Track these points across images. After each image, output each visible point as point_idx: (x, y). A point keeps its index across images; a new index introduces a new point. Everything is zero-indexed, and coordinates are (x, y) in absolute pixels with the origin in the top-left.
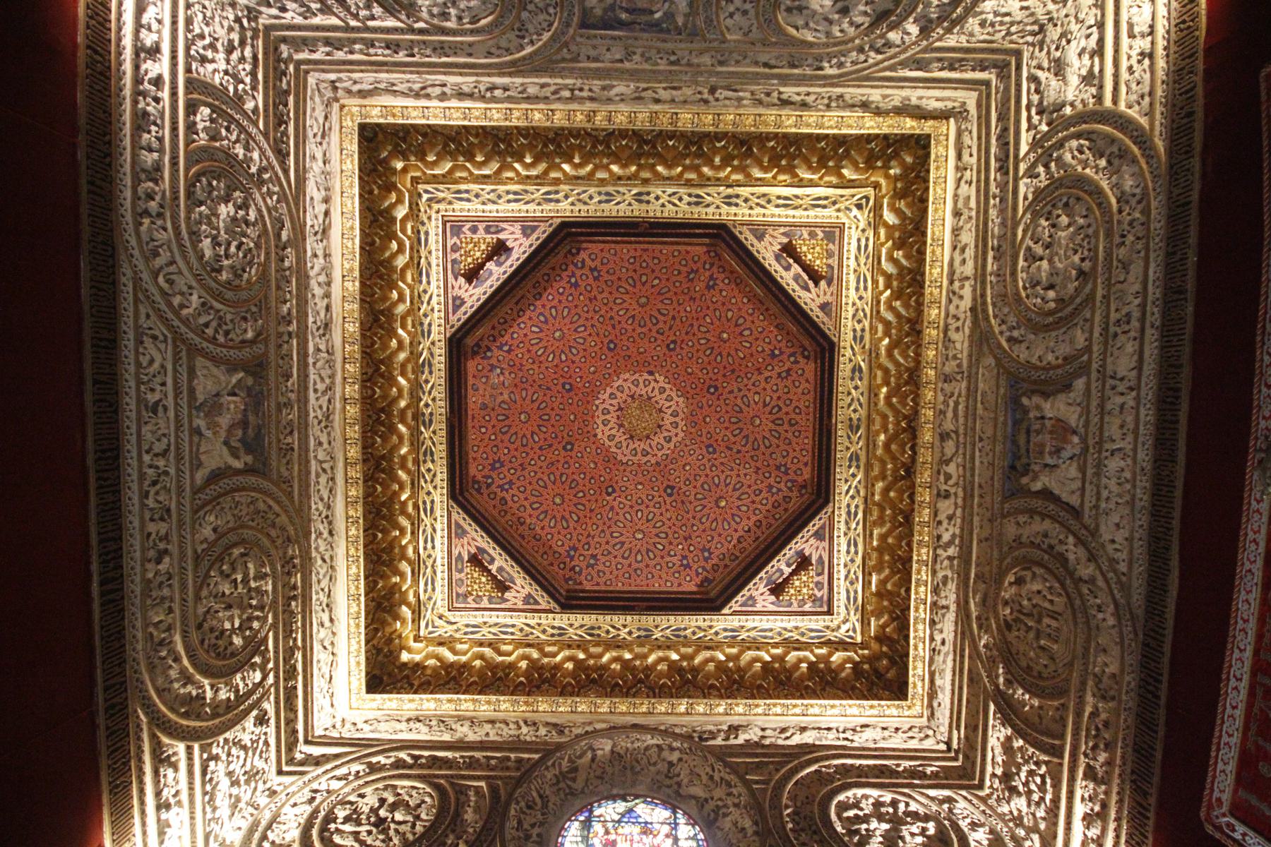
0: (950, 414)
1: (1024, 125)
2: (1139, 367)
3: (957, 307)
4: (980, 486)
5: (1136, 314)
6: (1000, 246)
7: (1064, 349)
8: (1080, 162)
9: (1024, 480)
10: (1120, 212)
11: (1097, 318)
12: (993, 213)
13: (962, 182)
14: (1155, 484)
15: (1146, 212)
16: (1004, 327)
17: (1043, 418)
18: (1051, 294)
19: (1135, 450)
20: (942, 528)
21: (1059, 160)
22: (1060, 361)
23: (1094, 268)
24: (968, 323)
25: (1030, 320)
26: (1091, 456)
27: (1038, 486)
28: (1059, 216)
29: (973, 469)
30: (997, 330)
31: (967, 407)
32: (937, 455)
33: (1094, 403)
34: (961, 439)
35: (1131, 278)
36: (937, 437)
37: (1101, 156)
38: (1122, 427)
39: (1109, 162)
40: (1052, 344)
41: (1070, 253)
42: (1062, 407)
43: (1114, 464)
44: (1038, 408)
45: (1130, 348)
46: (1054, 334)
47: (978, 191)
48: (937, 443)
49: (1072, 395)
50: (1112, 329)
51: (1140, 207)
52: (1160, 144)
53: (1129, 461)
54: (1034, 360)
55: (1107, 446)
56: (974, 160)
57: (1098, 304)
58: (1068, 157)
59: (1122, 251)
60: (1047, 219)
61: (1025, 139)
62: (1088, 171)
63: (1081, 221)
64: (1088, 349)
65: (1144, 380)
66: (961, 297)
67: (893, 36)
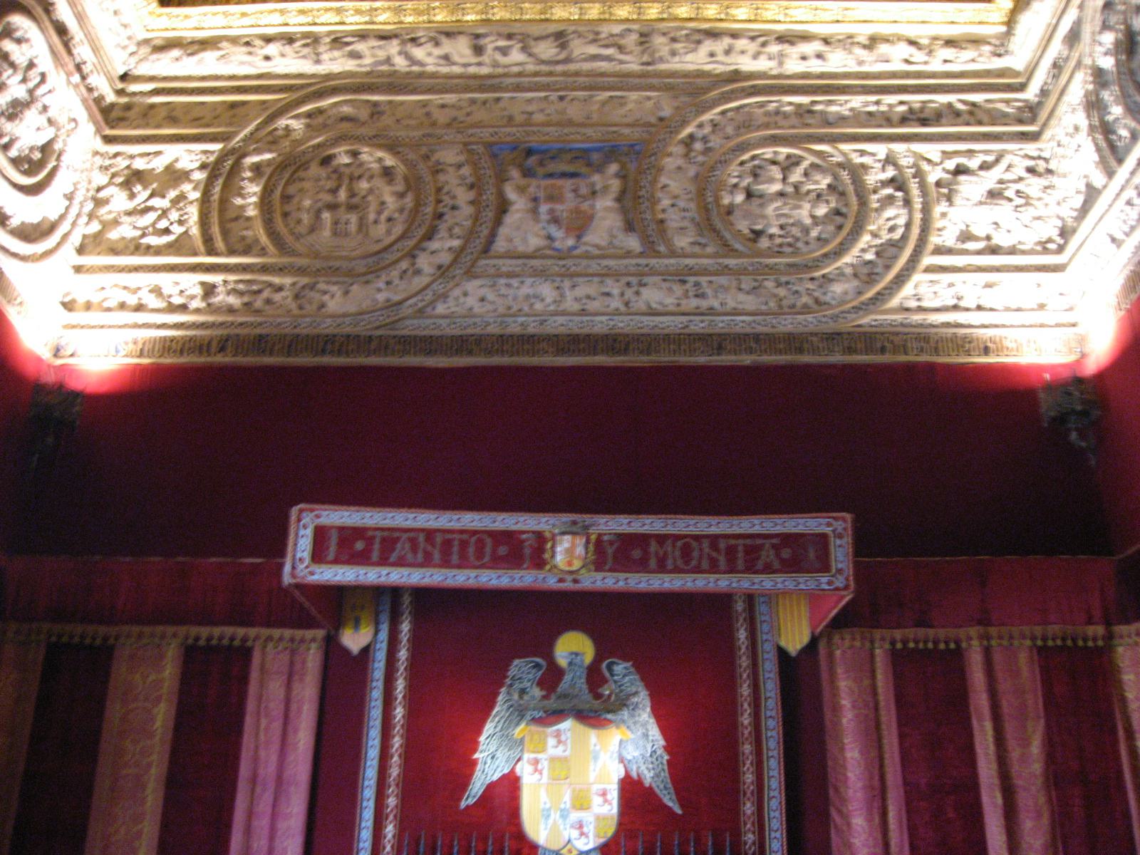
0: (593, 50)
1: (950, 147)
2: (652, 313)
3: (743, 52)
4: (498, 100)
5: (704, 304)
6: (810, 112)
7: (674, 220)
8: (879, 229)
9: (515, 173)
10: (812, 279)
11: (705, 261)
12: (857, 102)
13: (912, 50)
14: (533, 336)
15: (806, 309)
16: (707, 130)
17: (594, 193)
18: (740, 198)
19: (564, 313)
20: (429, 47)
21: (890, 200)
22: (660, 216)
23: (760, 254)
24: (720, 69)
25: (713, 169)
26: (552, 263)
27: (511, 194)
28: (827, 202)
29: (518, 88)
30: (706, 117)
31: (603, 75)
32: (536, 30)
33: (611, 263)
34: (560, 68)
35: (741, 297)
36: (560, 27)
37: (877, 254)
38: (588, 297)
39: (870, 262)
40: (682, 204)
41: (783, 221)
42: (608, 223)
43: (547, 291)
44: (606, 189)
45: (670, 301)
46: (692, 206)
47: (894, 75)
48: (552, 28)
49: (621, 236)
50: (692, 279)
51: (809, 301)
52: (866, 320)
53: (552, 308)
54: (663, 180)
55: (567, 284)
56: (936, 65)
57: (721, 261)
58: (890, 212)
59: (770, 284)
60: (829, 186)
61: (932, 150)
62: (866, 239)
63: (814, 233)
64: (673, 253)
65: (637, 318)
66: (756, 56)
67: (1109, 38)
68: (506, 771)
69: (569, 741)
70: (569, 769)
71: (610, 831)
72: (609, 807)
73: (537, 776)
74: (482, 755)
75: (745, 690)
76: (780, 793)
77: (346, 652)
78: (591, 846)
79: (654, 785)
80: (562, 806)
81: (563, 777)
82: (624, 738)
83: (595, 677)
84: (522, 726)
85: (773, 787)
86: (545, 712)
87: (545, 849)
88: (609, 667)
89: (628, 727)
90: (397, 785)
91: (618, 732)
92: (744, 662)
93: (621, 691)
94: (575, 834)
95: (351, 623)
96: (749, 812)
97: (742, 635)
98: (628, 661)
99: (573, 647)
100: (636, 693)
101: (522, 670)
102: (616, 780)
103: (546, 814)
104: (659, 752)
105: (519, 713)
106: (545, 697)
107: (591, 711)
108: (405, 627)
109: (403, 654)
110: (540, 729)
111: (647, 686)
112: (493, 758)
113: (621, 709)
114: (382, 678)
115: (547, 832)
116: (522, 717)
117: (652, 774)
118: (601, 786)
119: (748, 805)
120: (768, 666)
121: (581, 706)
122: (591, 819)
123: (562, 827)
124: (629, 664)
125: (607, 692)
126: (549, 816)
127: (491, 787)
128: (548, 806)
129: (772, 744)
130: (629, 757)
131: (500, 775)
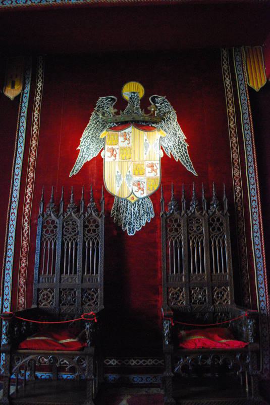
68: (95, 156)
69: (131, 139)
70: (131, 154)
71: (156, 187)
72: (153, 174)
73: (113, 158)
74: (82, 148)
75: (231, 109)
76: (254, 163)
77: (8, 98)
78: (145, 195)
79: (180, 160)
80: (128, 173)
81: (128, 157)
82: (163, 136)
83: (144, 103)
84: (105, 131)
85: (250, 161)
86: (117, 123)
87: (118, 197)
88: (153, 100)
89: (165, 130)
90: (34, 167)
91: (159, 133)
92: (230, 95)
93: (160, 112)
94: (135, 188)
95: (10, 86)
96: (237, 174)
97: (228, 81)
98: (163, 96)
99: (132, 90)
100: (169, 112)
101: (106, 104)
102: (158, 159)
103: (119, 178)
104: (183, 143)
105: (104, 125)
106: (117, 113)
107: (143, 122)
108: (40, 85)
109: (38, 98)
110: (114, 133)
111: (175, 109)
112: (87, 149)
113: (161, 121)
114: (26, 111)
115: (118, 188)
116: (105, 127)
117: (179, 155)
118: (151, 162)
119: (236, 170)
120: (243, 97)
121: (137, 119)
122: (145, 180)
123: (127, 185)
124: (164, 98)
125: (153, 109)
126: (120, 179)
127: (87, 164)
128: (119, 174)
129: (248, 137)
130: (166, 146)
131: (92, 158)
